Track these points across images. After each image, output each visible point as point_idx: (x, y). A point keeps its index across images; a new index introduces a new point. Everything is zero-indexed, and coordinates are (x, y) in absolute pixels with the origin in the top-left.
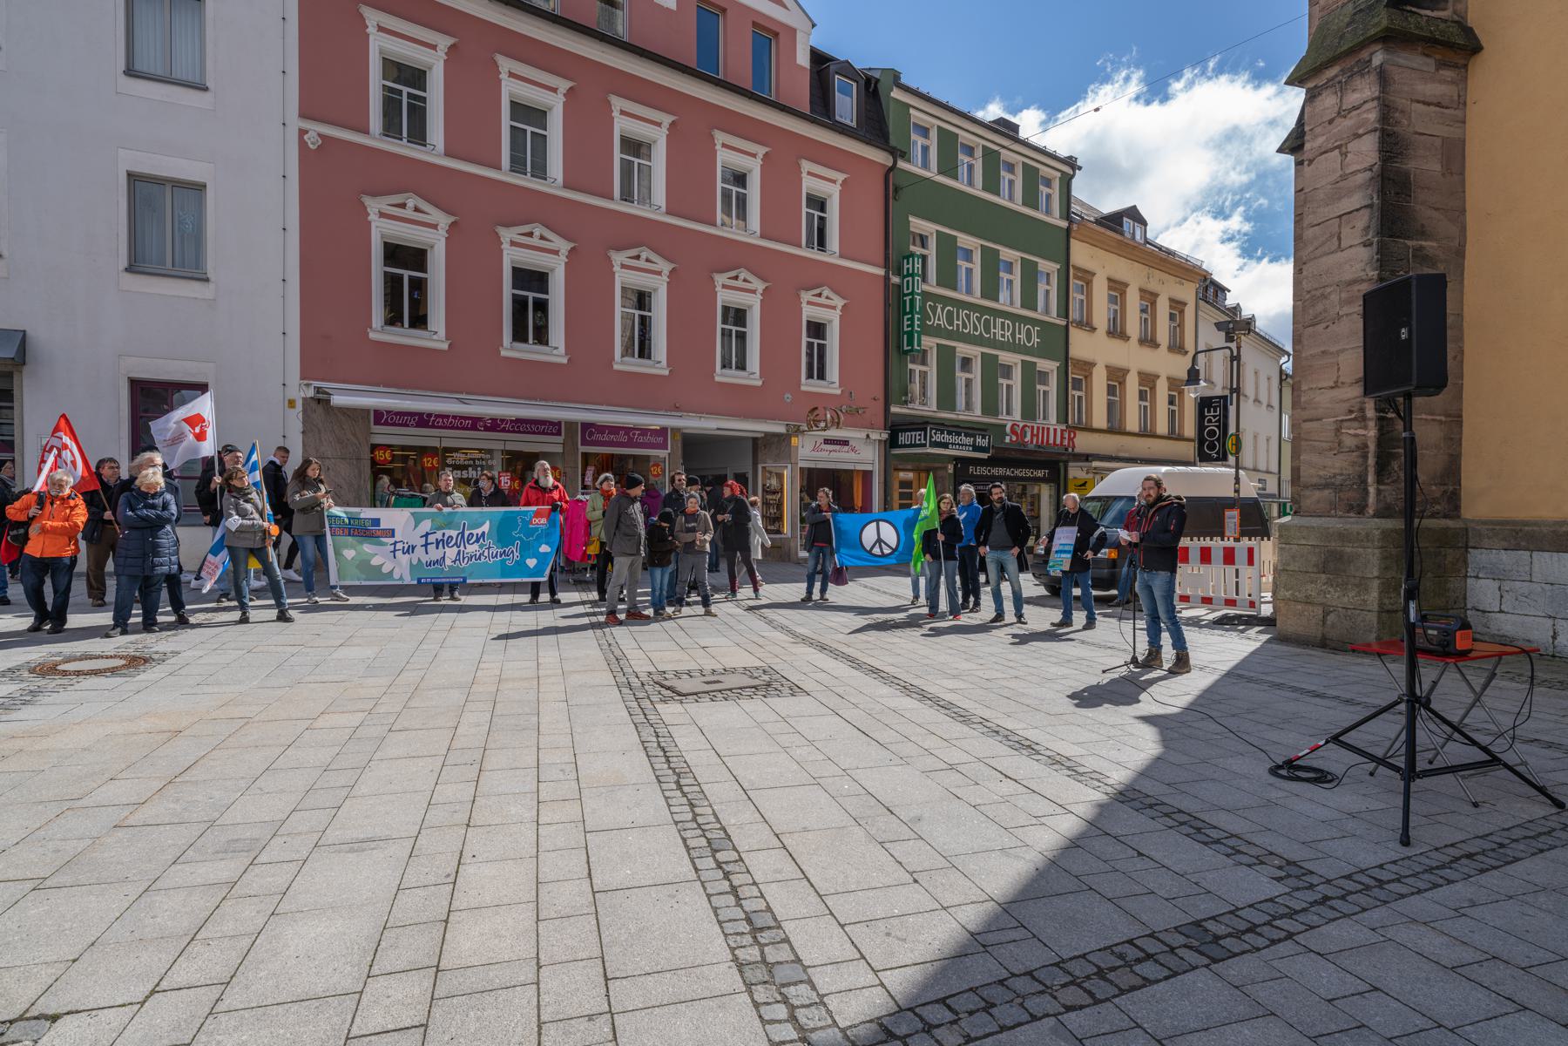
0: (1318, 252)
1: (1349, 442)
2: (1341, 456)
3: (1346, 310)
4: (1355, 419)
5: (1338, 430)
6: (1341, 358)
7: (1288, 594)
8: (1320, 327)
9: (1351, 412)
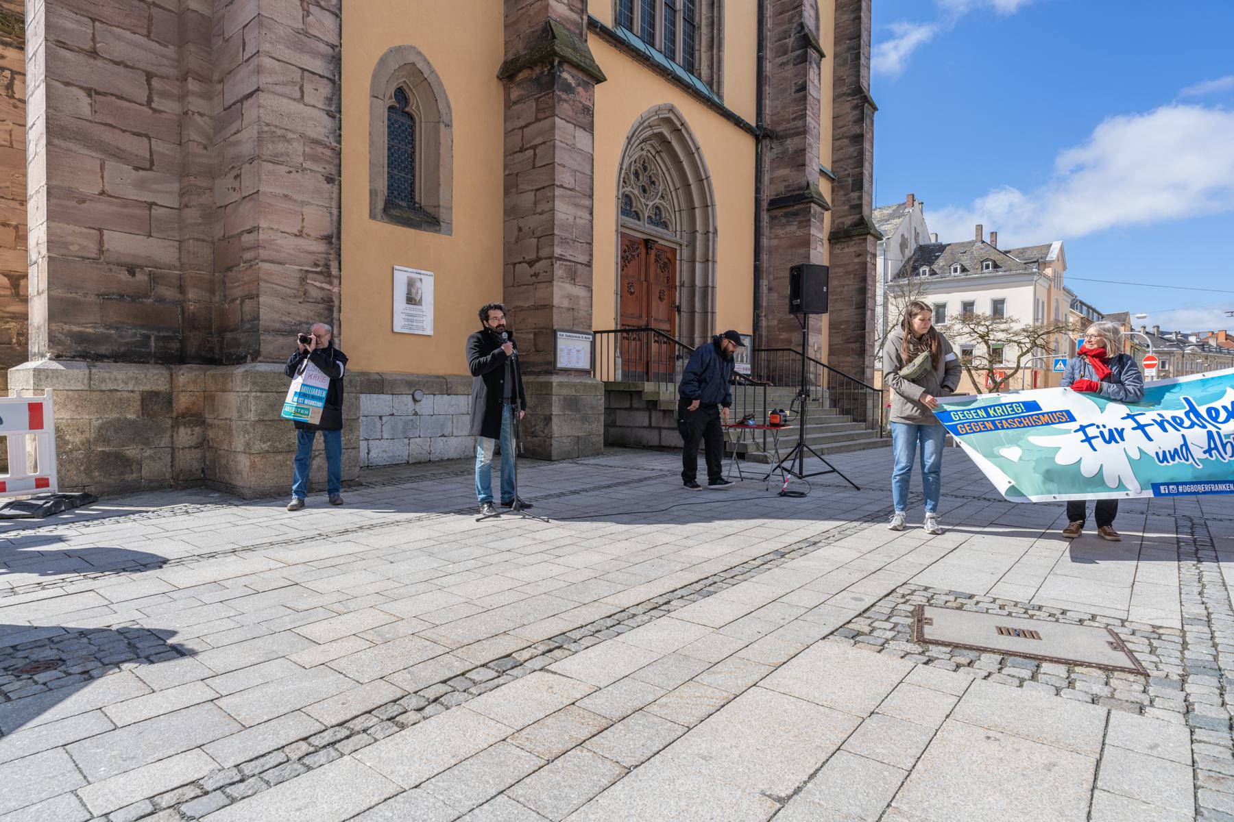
0: (278, 89)
1: (315, 293)
3: (308, 165)
4: (320, 273)
5: (303, 280)
6: (306, 210)
7: (265, 446)
8: (282, 169)
9: (317, 265)
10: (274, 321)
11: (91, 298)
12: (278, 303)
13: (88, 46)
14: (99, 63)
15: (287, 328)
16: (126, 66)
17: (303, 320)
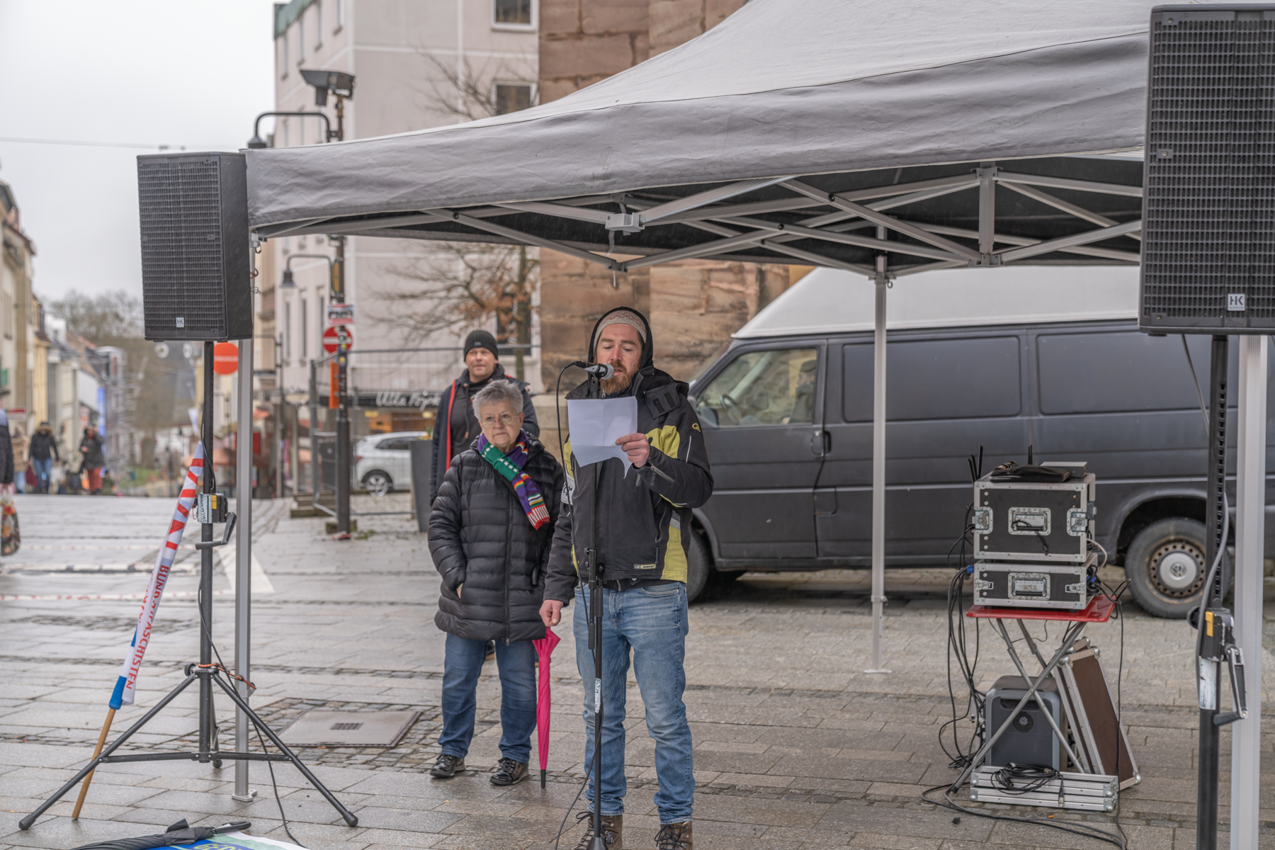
1: (721, 299)
2: (711, 317)
5: (705, 282)
10: (668, 343)
11: (577, 321)
12: (672, 318)
13: (573, 29)
14: (585, 42)
15: (685, 350)
16: (610, 34)
17: (705, 337)
